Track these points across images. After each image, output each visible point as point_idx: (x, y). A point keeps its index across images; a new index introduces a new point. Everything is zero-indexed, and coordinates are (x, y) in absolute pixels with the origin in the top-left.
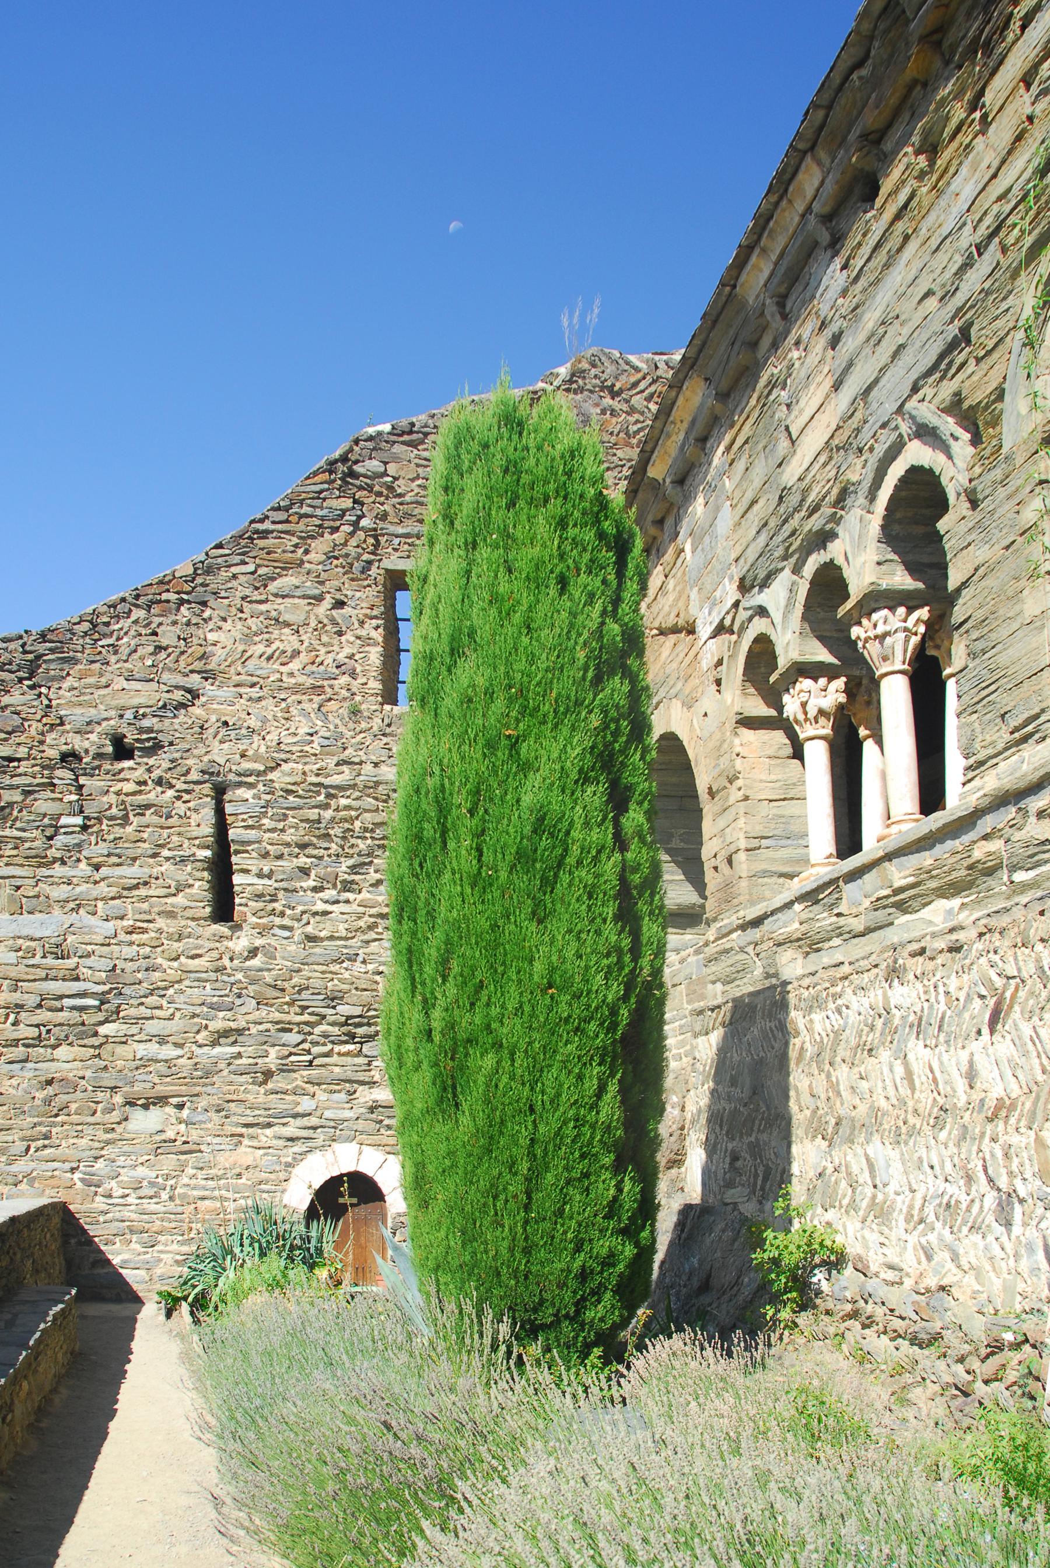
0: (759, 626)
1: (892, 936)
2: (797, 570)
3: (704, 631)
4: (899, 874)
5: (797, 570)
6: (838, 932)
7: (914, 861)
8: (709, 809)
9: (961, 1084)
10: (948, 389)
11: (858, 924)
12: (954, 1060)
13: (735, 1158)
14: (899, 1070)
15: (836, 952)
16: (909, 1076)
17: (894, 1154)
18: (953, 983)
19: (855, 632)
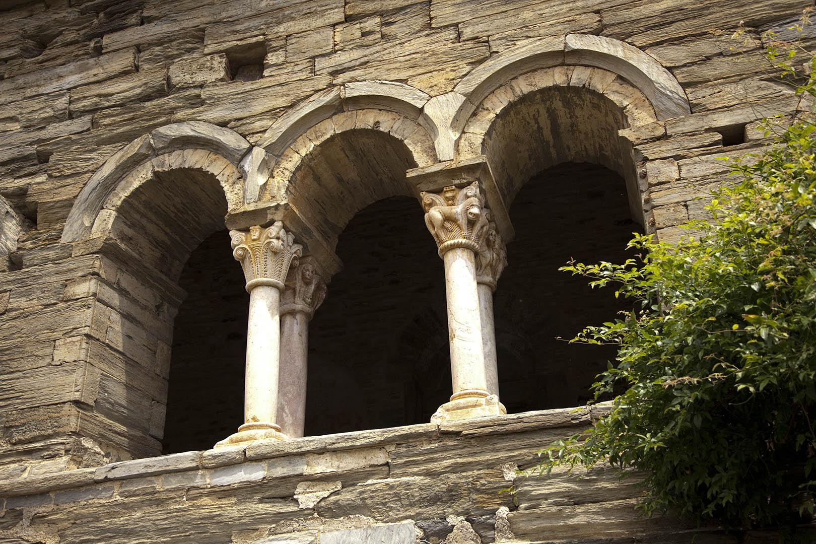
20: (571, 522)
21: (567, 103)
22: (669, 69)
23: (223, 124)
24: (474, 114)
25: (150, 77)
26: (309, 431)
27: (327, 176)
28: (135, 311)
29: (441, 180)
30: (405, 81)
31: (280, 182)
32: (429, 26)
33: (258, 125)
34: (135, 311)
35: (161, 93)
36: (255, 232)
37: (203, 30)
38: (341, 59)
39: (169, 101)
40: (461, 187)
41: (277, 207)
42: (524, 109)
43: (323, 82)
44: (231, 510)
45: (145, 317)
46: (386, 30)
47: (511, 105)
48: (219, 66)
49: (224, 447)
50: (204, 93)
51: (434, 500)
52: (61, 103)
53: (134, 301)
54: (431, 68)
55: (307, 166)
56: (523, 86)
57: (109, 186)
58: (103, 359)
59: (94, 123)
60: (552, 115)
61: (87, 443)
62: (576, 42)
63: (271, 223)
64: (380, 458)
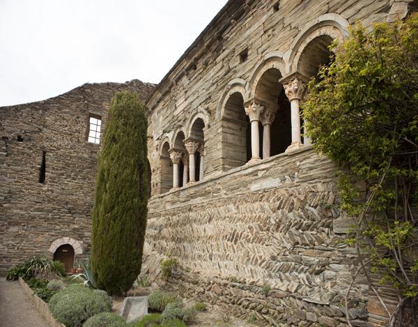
0: (166, 140)
1: (189, 203)
2: (175, 131)
3: (155, 139)
4: (192, 191)
5: (175, 131)
6: (179, 201)
7: (195, 189)
8: (153, 174)
9: (203, 232)
10: (206, 106)
11: (183, 200)
12: (201, 228)
13: (155, 245)
14: (191, 229)
15: (178, 205)
16: (192, 230)
17: (189, 245)
18: (202, 213)
19: (186, 145)
20: (310, 174)
21: (323, 40)
22: (347, 19)
23: (240, 78)
24: (296, 54)
25: (226, 68)
26: (271, 155)
27: (267, 83)
28: (234, 132)
30: (278, 50)
31: (253, 91)
32: (283, 27)
33: (247, 75)
34: (234, 132)
35: (228, 72)
38: (264, 47)
39: (230, 74)
42: (311, 47)
43: (260, 56)
44: (248, 179)
45: (238, 133)
46: (274, 33)
47: (306, 48)
48: (238, 58)
49: (247, 164)
50: (236, 69)
51: (282, 173)
52: (211, 82)
53: (233, 129)
55: (260, 83)
56: (308, 40)
57: (222, 102)
58: (227, 146)
59: (217, 85)
60: (321, 44)
61: (226, 166)
62: (321, 19)
64: (273, 163)
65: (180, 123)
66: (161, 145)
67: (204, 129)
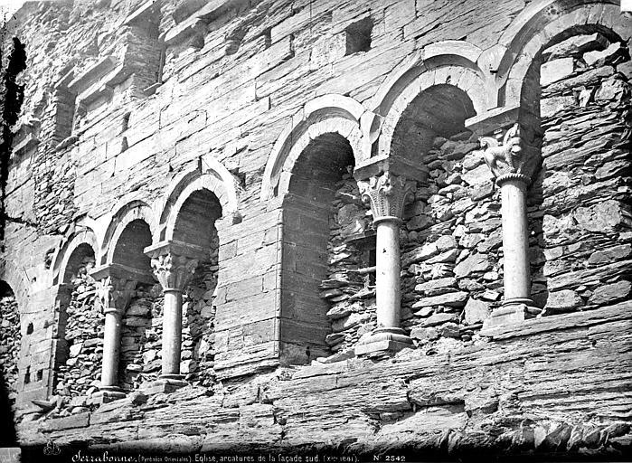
29: (491, 126)
33: (368, 93)
36: (373, 180)
37: (331, 13)
40: (507, 128)
41: (383, 161)
54: (482, 24)
63: (382, 173)
65: (138, 195)
66: (61, 252)
67: (218, 224)
